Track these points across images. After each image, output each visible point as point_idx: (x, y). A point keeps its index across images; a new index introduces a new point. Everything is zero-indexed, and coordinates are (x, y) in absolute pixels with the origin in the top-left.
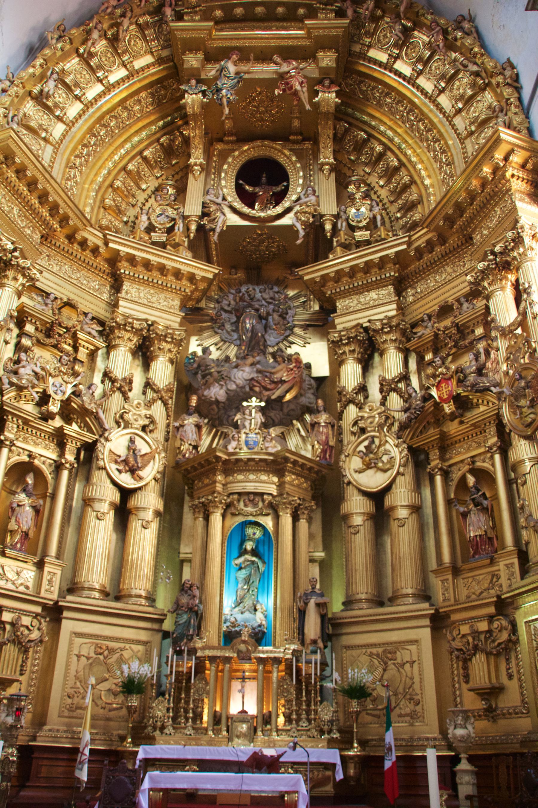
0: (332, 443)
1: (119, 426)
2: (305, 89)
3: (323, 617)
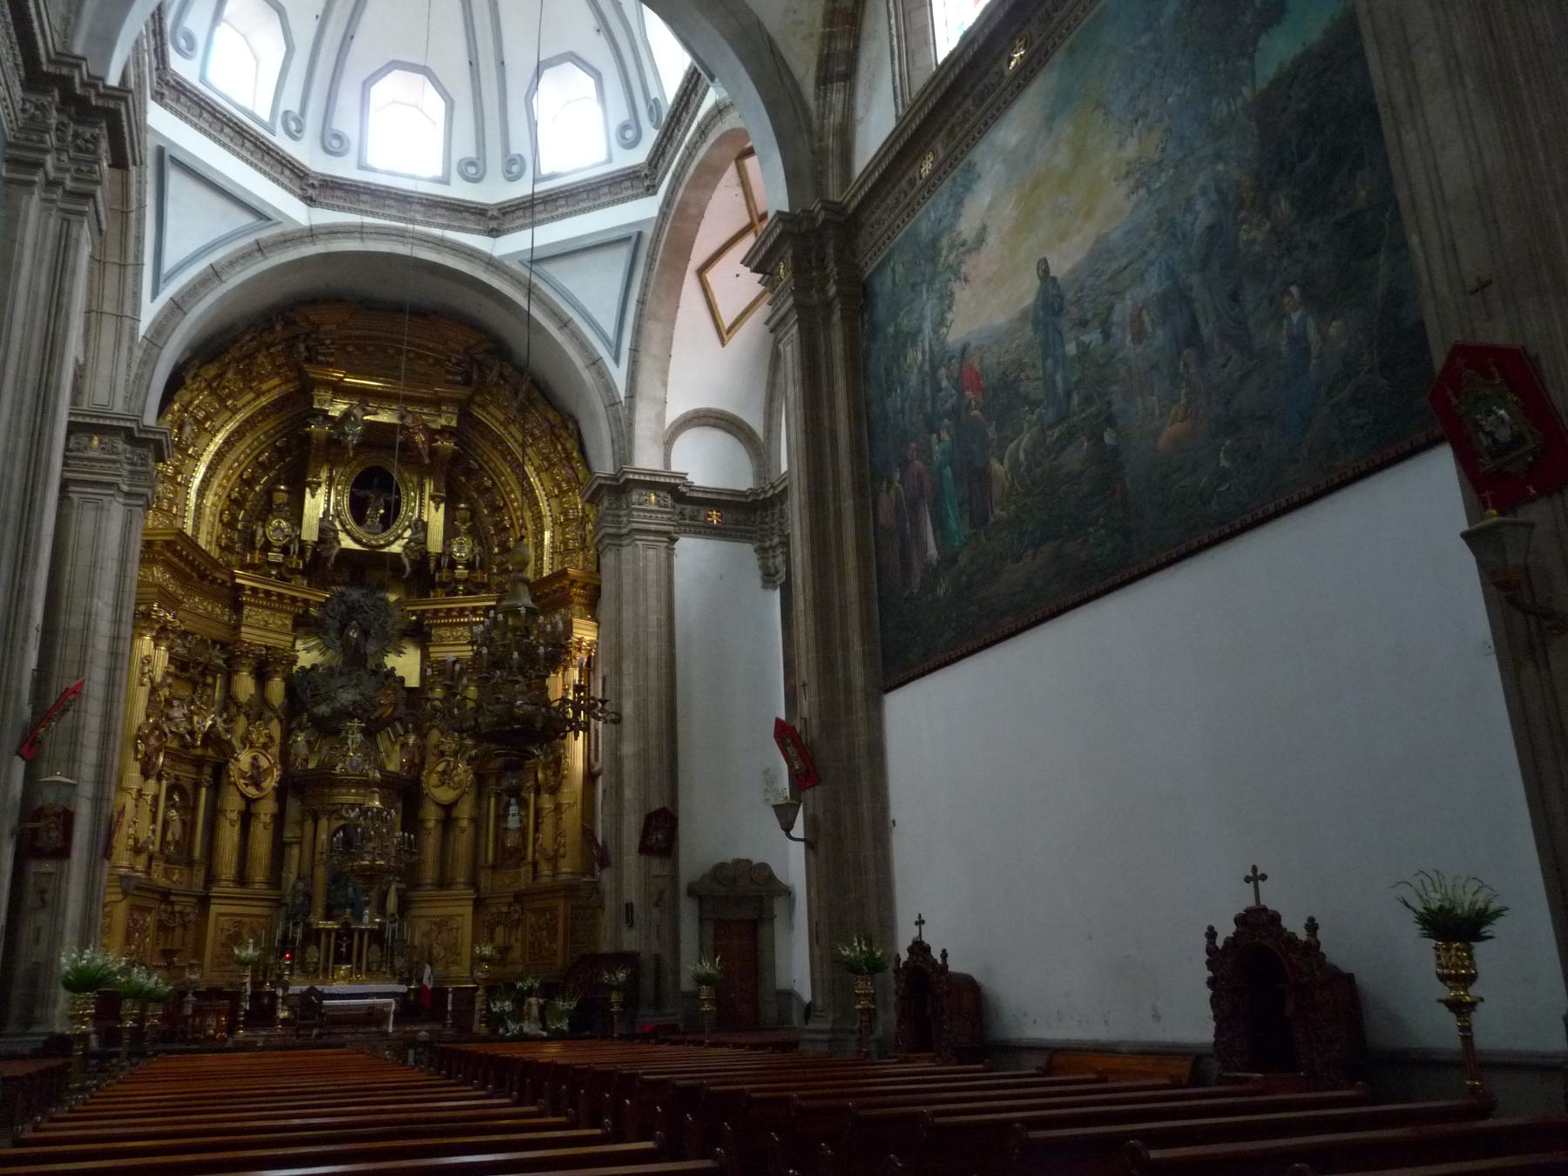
0: (417, 760)
1: (245, 747)
2: (426, 446)
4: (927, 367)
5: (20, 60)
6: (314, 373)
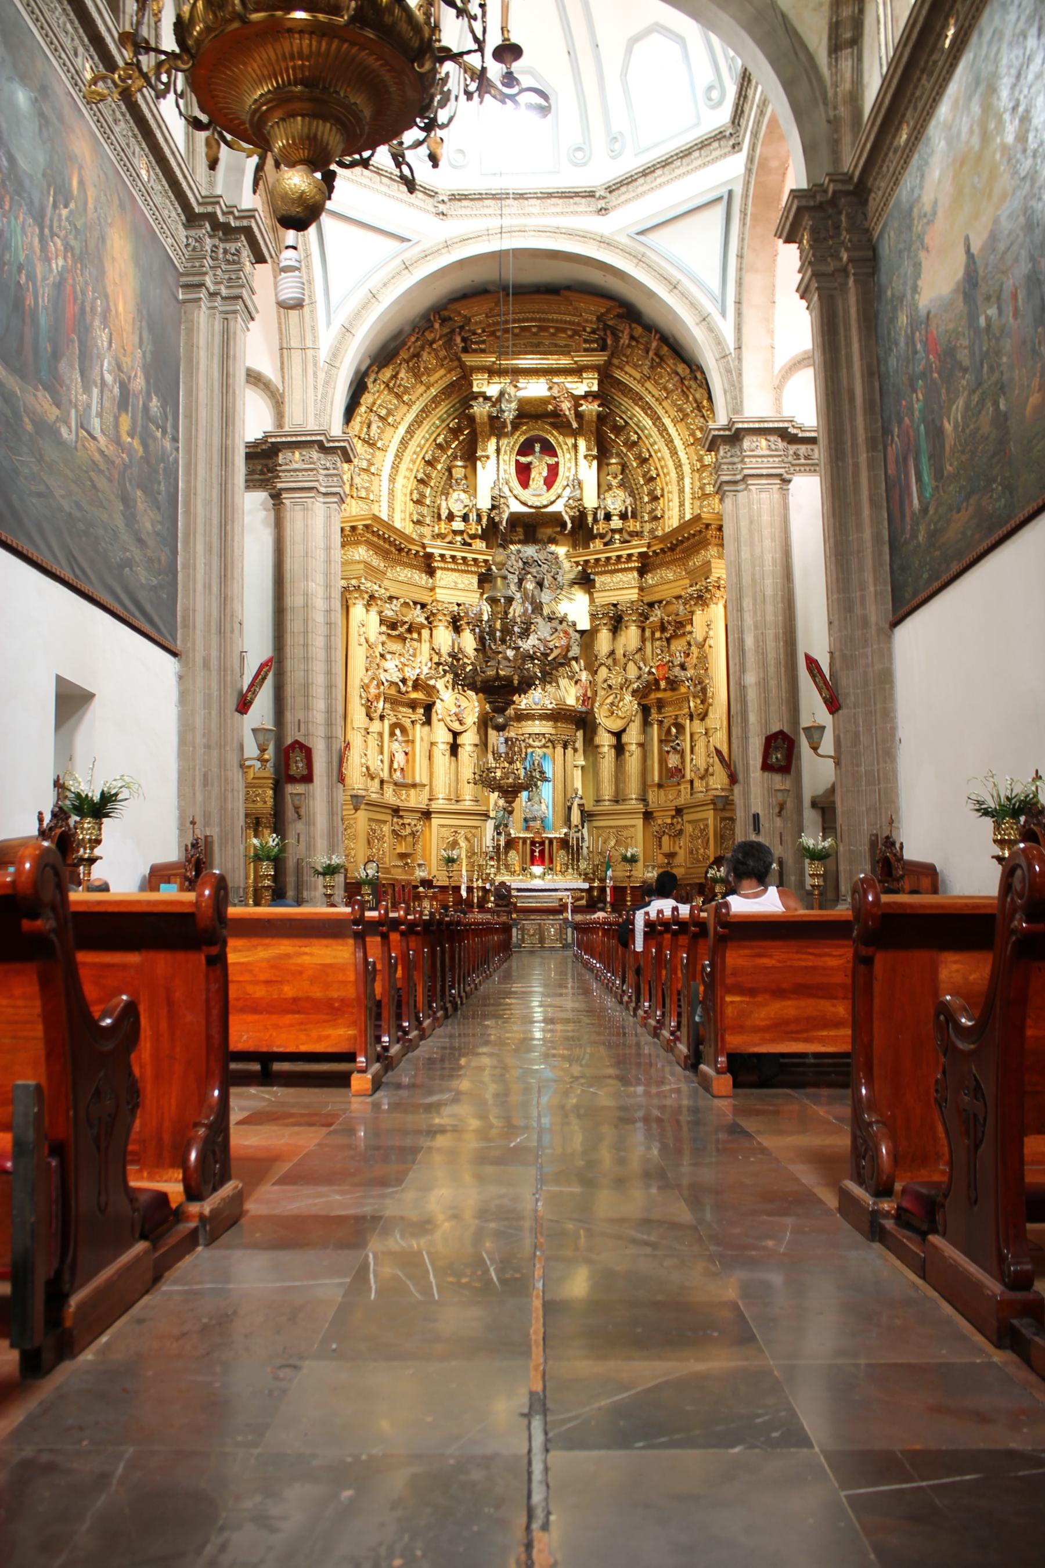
0: (589, 694)
3: (582, 812)
4: (909, 331)
5: (180, 210)
6: (470, 360)
